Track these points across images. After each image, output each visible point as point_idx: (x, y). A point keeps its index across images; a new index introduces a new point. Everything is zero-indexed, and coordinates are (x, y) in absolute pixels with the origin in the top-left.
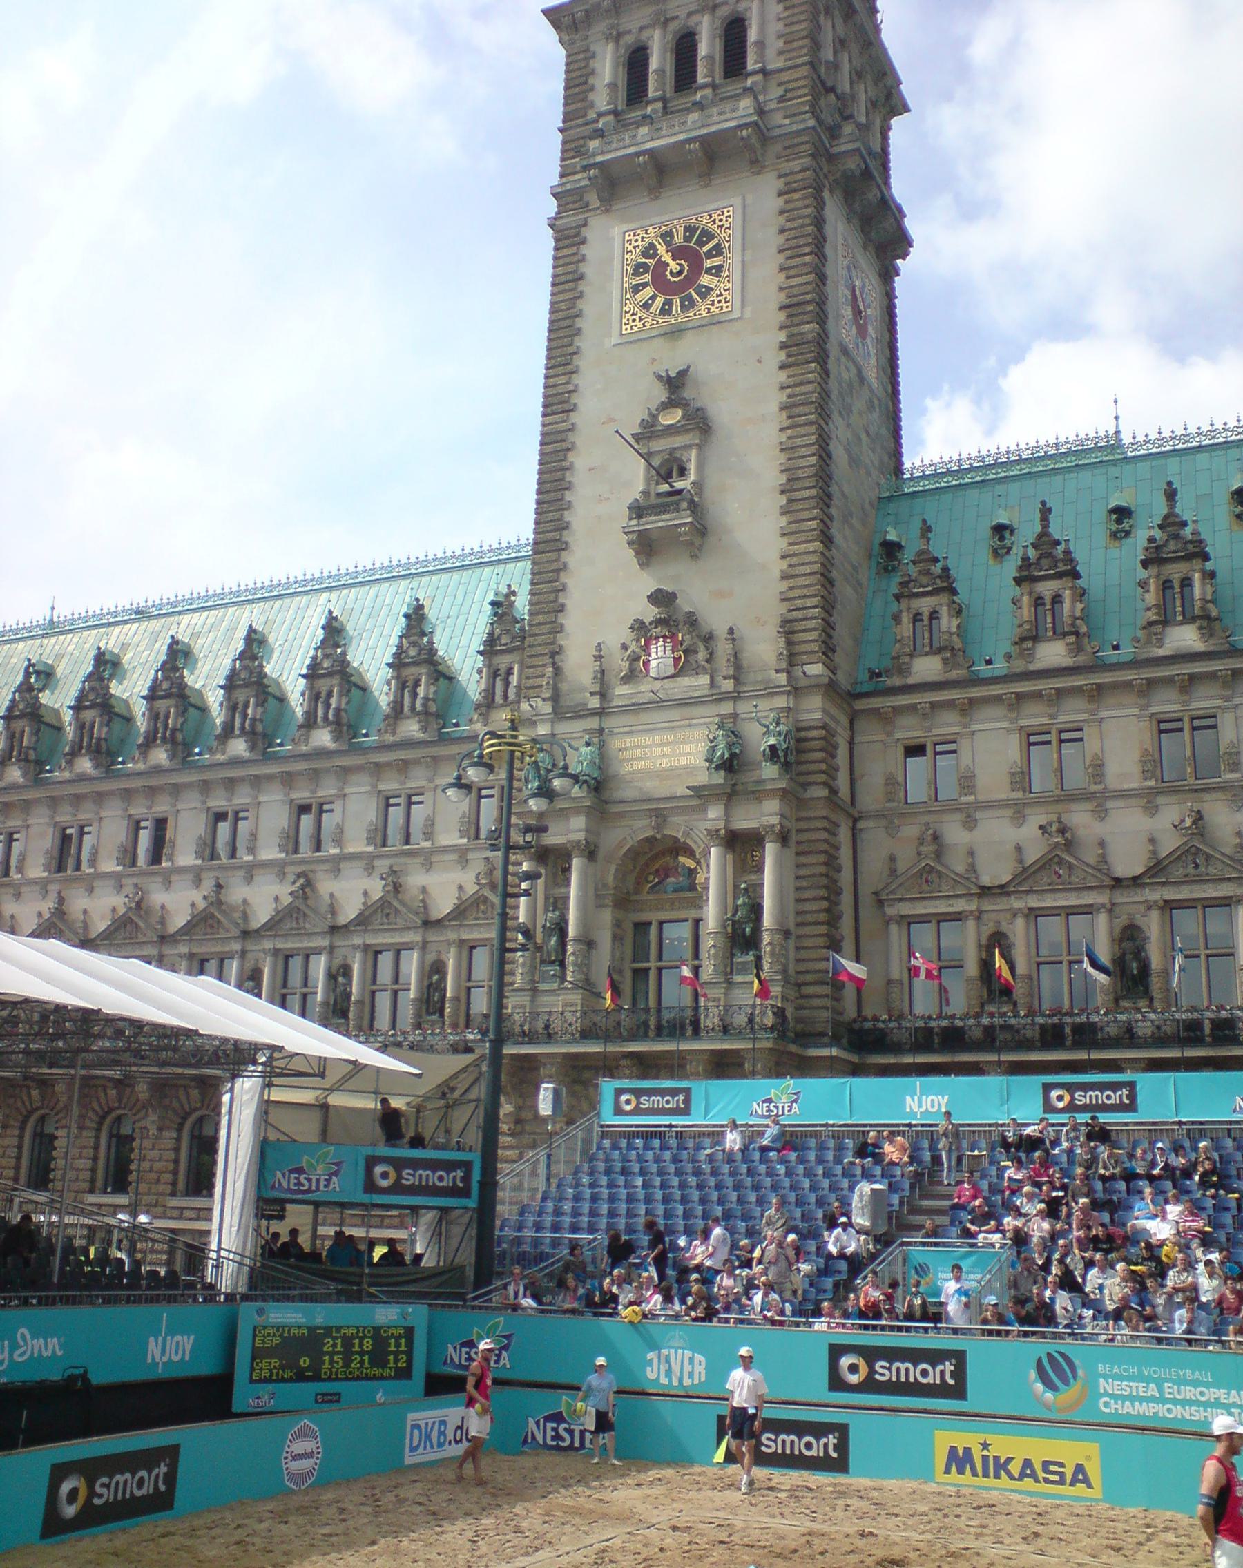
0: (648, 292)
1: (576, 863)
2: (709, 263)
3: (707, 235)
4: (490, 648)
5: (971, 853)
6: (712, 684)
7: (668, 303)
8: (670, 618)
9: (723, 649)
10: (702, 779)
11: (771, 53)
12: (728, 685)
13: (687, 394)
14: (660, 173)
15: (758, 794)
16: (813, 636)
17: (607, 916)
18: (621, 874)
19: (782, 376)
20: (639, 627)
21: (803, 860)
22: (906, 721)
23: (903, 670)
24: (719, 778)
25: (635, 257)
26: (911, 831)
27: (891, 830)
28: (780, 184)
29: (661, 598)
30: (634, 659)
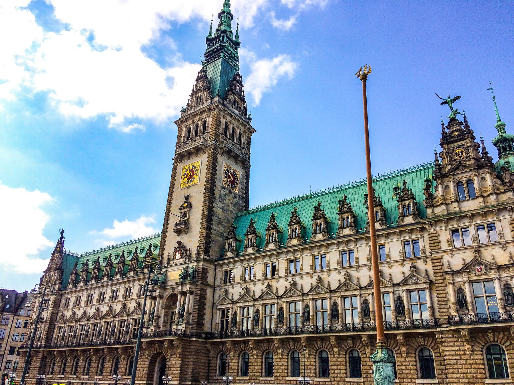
2: (195, 173)
5: (233, 294)
6: (186, 260)
10: (178, 281)
11: (209, 128)
13: (189, 200)
14: (189, 154)
16: (202, 249)
20: (175, 249)
21: (197, 297)
22: (225, 266)
23: (226, 255)
25: (184, 172)
26: (223, 290)
28: (208, 156)
29: (179, 243)
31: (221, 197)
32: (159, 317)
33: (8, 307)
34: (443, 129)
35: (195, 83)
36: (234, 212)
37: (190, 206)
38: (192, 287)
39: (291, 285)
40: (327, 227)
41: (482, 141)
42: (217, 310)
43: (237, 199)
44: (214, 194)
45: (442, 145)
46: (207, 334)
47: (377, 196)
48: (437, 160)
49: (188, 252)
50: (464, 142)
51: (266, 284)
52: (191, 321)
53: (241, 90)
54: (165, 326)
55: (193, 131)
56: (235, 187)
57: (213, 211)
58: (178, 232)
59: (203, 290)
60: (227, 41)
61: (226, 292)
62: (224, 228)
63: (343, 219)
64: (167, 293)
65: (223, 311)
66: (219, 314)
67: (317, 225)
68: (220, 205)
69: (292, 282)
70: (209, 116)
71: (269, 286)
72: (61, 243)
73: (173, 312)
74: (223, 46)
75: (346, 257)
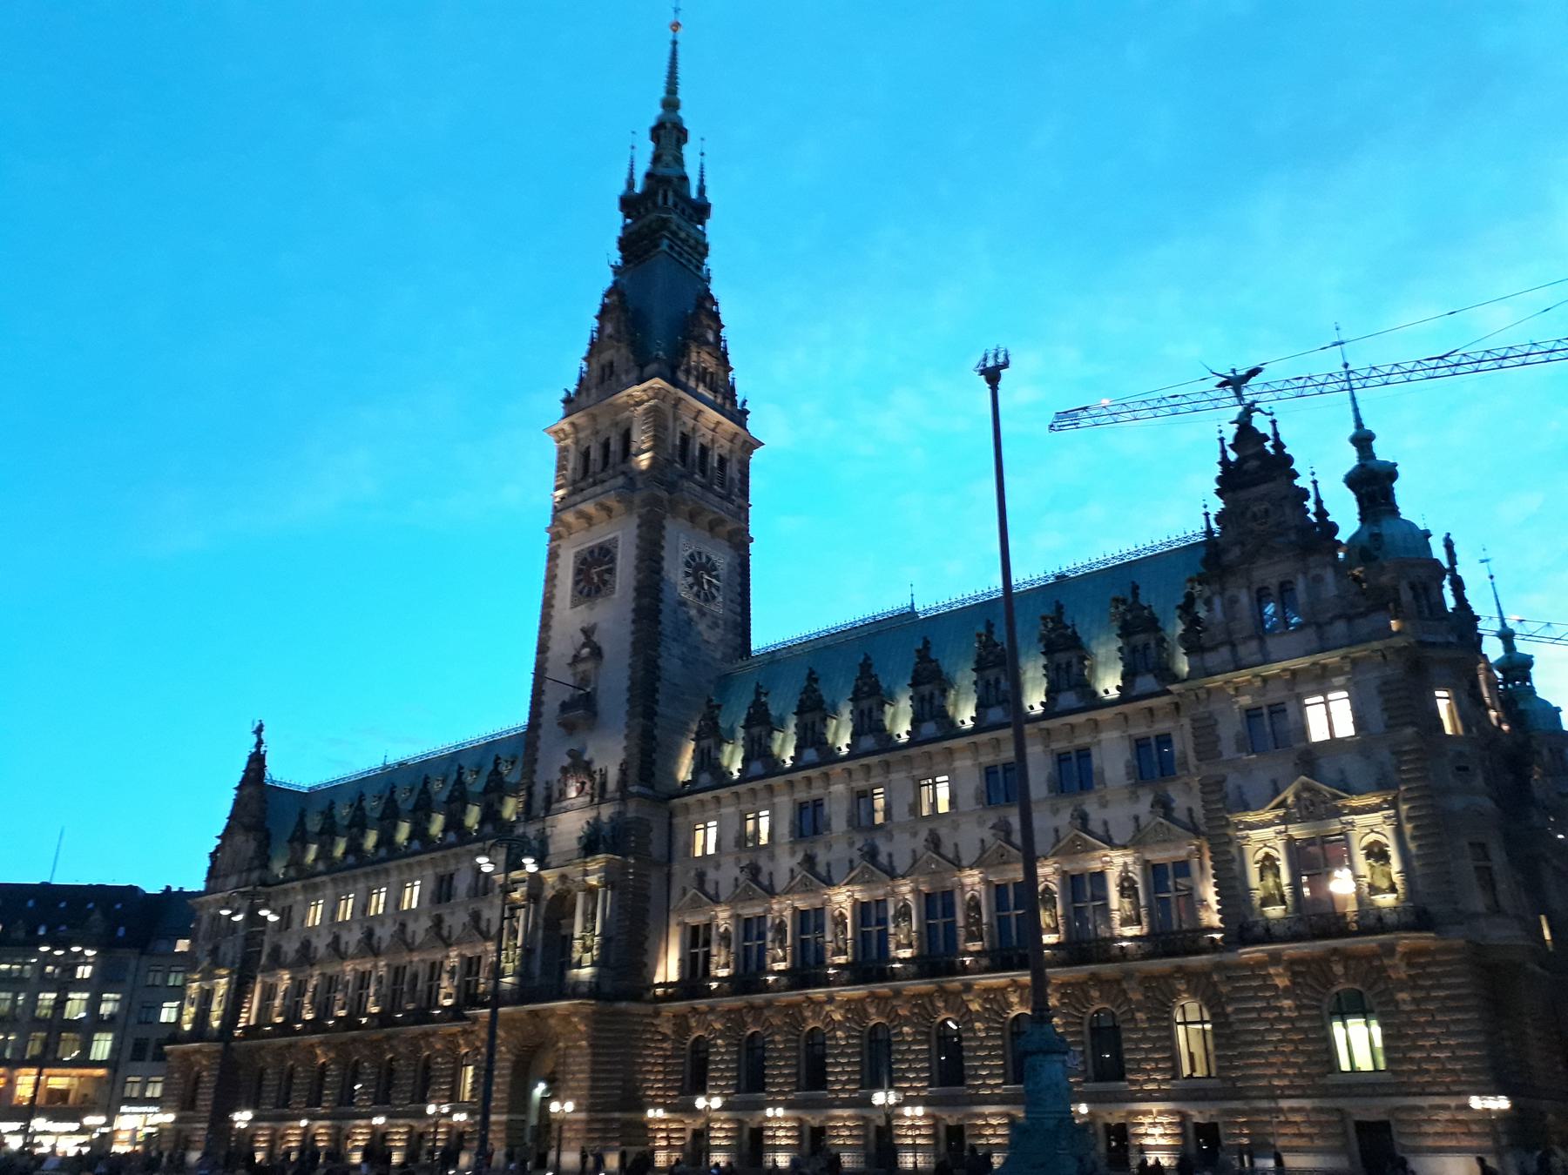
29: (573, 754)
33: (121, 931)
34: (1224, 452)
35: (596, 323)
37: (597, 653)
41: (1315, 482)
43: (720, 631)
45: (1219, 493)
47: (1069, 623)
48: (1209, 532)
49: (597, 777)
50: (1271, 485)
51: (800, 857)
53: (718, 339)
56: (714, 597)
57: (658, 667)
58: (569, 728)
60: (675, 205)
68: (676, 649)
72: (257, 762)
74: (666, 221)
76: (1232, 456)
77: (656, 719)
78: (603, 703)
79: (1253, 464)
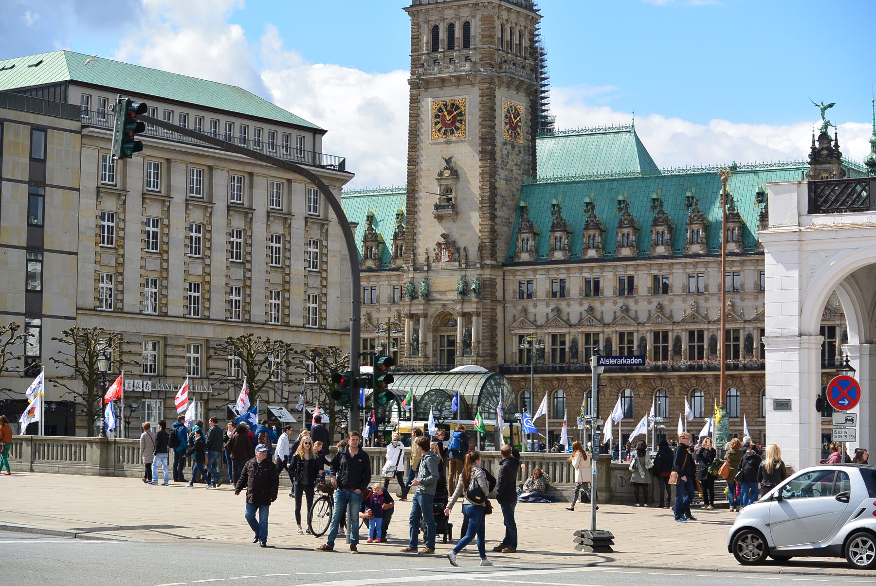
0: (440, 125)
1: (421, 320)
3: (458, 108)
4: (396, 236)
5: (535, 315)
6: (460, 265)
7: (446, 130)
8: (448, 243)
9: (462, 253)
12: (463, 266)
13: (452, 165)
15: (470, 302)
17: (430, 335)
18: (435, 322)
19: (480, 164)
20: (439, 244)
23: (519, 258)
24: (460, 297)
26: (520, 308)
27: (515, 307)
28: (480, 92)
30: (437, 254)
31: (503, 161)
32: (426, 343)
34: (814, 142)
36: (519, 178)
37: (455, 173)
38: (479, 306)
39: (623, 311)
40: (670, 239)
42: (513, 335)
44: (495, 160)
46: (501, 367)
51: (586, 306)
52: (481, 352)
54: (434, 355)
55: (443, 35)
57: (495, 188)
58: (440, 218)
59: (493, 310)
61: (525, 311)
62: (509, 209)
63: (693, 231)
64: (435, 309)
65: (521, 338)
66: (516, 340)
67: (658, 233)
69: (624, 308)
70: (474, 17)
71: (591, 309)
73: (442, 337)
75: (693, 281)
76: (817, 145)
77: (497, 220)
78: (463, 206)
79: (825, 152)
